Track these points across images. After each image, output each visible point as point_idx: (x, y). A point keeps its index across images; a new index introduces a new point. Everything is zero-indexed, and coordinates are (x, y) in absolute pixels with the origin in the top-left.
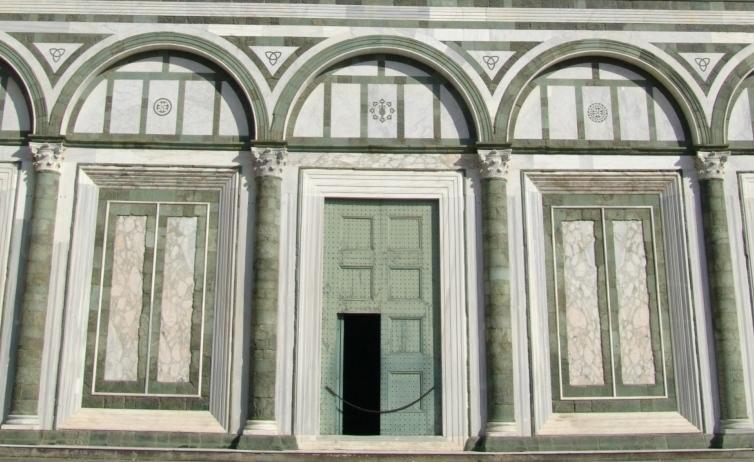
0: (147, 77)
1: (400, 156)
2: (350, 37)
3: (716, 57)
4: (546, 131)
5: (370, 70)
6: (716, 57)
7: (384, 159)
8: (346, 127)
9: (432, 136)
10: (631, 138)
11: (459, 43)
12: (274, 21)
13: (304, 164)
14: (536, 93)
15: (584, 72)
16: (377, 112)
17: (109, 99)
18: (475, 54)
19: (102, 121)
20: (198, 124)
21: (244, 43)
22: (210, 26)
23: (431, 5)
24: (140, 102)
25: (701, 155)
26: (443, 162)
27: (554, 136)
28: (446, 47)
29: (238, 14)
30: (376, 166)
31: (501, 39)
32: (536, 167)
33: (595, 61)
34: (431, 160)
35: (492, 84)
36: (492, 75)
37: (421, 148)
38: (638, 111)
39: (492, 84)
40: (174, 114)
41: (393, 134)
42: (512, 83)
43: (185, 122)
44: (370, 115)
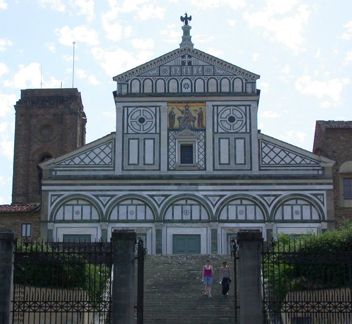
0: (127, 205)
1: (191, 224)
2: (178, 194)
3: (273, 198)
4: (228, 217)
5: (183, 202)
6: (273, 198)
7: (187, 225)
8: (178, 216)
9: (198, 218)
10: (250, 219)
11: (206, 195)
12: (159, 190)
13: (167, 226)
14: (226, 207)
15: (238, 202)
16: (185, 213)
17: (118, 211)
18: (209, 198)
19: (117, 217)
20: (141, 217)
21: (151, 196)
22: (143, 192)
23: (199, 185)
24: (126, 211)
25: (266, 223)
26: (202, 225)
27: (229, 219)
28: (203, 196)
29: (150, 189)
30: (185, 226)
31: (217, 194)
32: (225, 226)
33: (241, 199)
34: (199, 225)
35: (214, 206)
36: (214, 203)
37: (196, 221)
38: (252, 212)
39: (214, 206)
40: (135, 214)
41: (189, 218)
42: (219, 205)
43: (138, 216)
44: (184, 214)
